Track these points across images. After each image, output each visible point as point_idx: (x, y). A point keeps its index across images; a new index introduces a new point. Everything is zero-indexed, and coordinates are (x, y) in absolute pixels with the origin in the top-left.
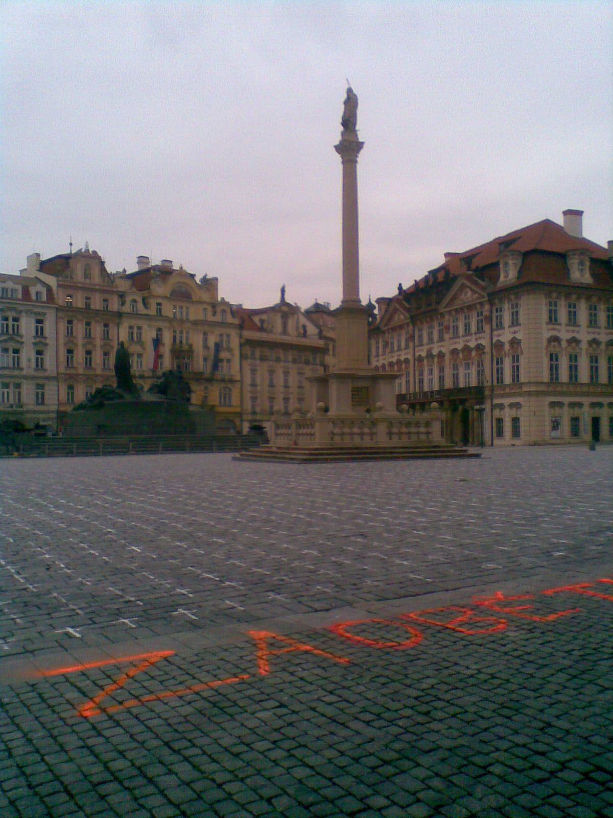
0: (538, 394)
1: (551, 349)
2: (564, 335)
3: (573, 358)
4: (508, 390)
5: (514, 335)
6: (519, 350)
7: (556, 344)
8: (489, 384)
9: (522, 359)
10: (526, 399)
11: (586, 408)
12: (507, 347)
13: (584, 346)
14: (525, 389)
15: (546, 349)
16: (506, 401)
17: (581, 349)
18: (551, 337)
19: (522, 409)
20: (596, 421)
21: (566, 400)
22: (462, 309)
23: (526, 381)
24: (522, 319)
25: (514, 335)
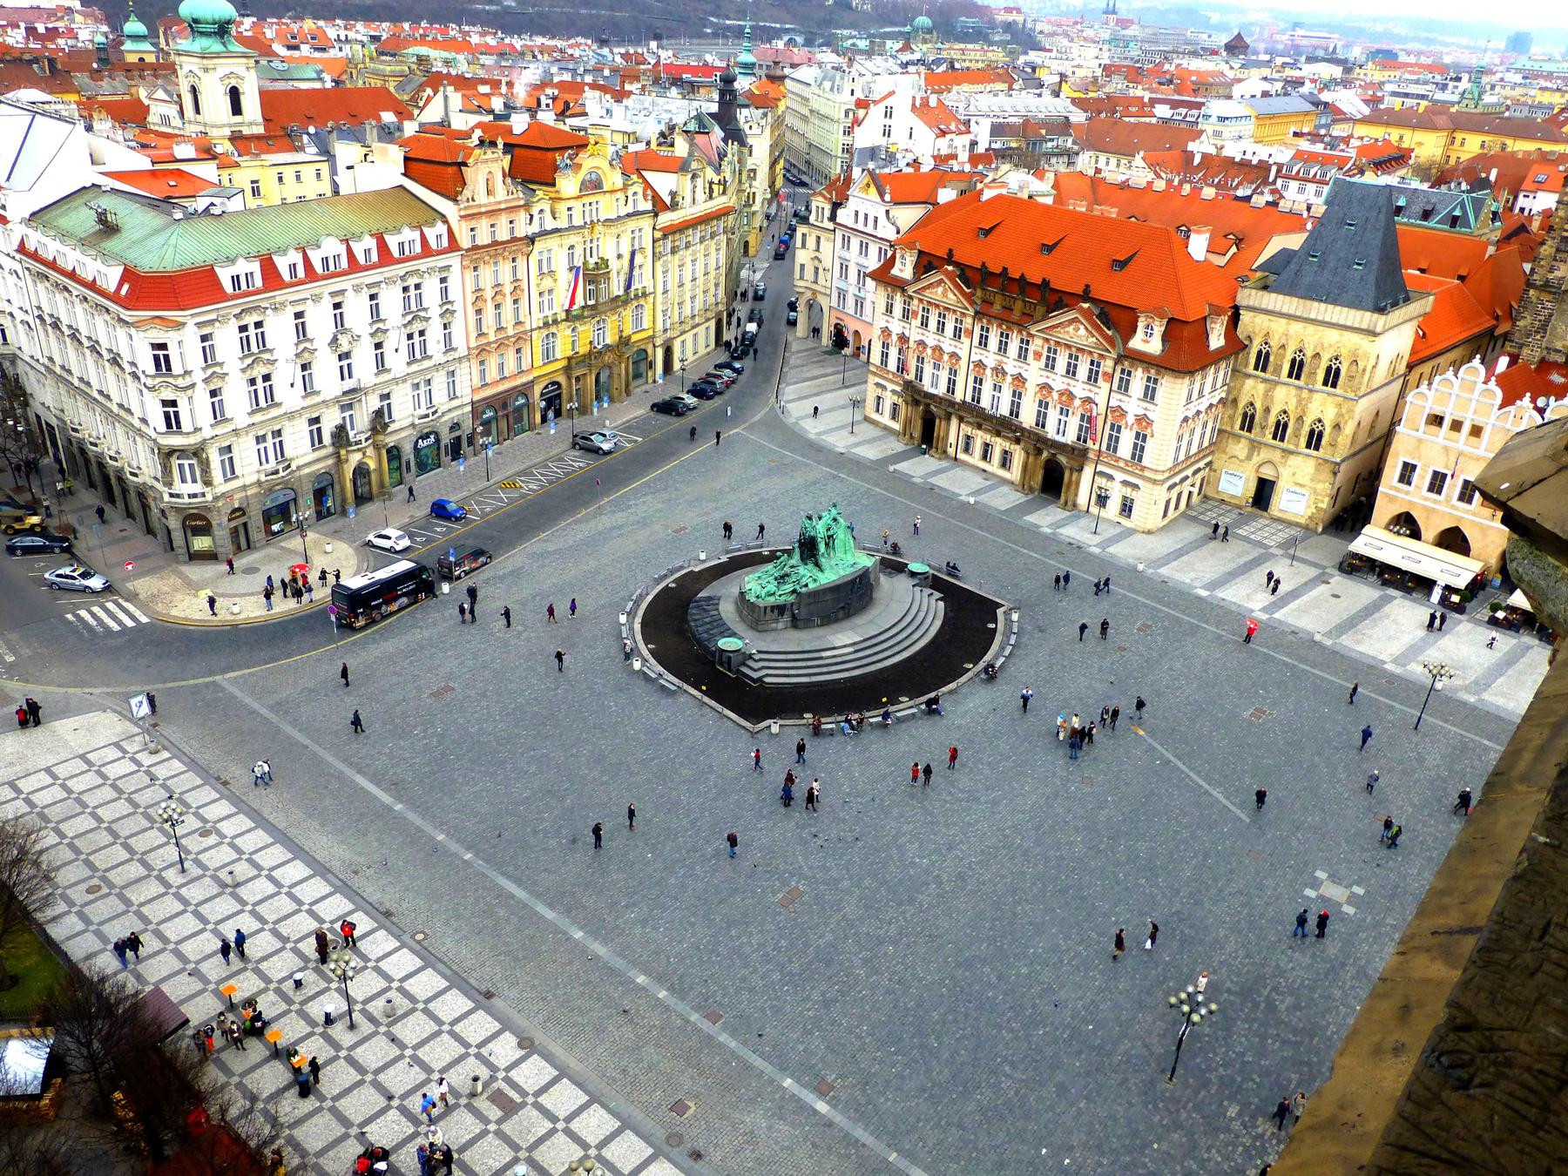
4: (1122, 464)
8: (1096, 447)
12: (1131, 419)
16: (1119, 476)
22: (1068, 346)
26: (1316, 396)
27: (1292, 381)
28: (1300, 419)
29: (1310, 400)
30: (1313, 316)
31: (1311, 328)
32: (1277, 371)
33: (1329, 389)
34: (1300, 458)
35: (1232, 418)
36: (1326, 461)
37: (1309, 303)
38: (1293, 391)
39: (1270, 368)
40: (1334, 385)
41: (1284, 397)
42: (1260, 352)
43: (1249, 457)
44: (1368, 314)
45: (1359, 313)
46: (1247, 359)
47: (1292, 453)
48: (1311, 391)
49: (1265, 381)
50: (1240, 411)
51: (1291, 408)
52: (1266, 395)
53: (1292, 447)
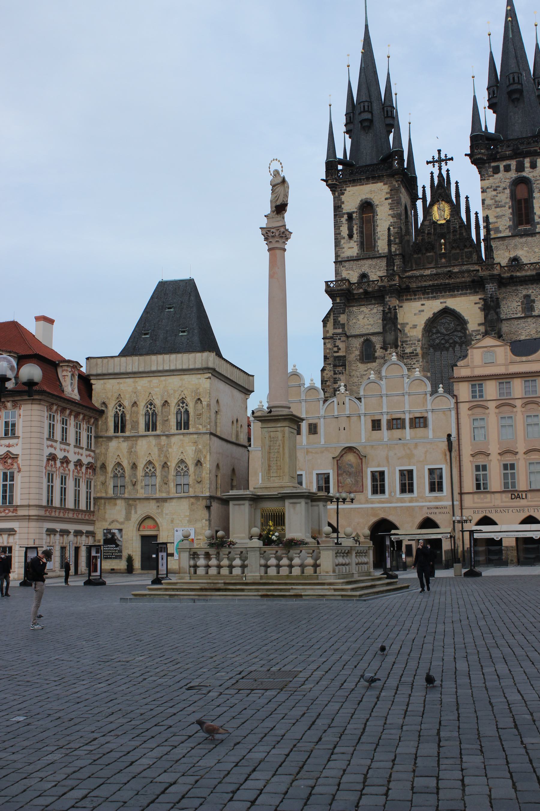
0: (40, 519)
1: (48, 468)
2: (60, 455)
3: (63, 480)
5: (8, 449)
6: (15, 466)
7: (53, 463)
9: (18, 478)
10: (25, 524)
11: (71, 537)
13: (71, 466)
14: (21, 512)
15: (45, 468)
17: (69, 470)
18: (51, 454)
19: (17, 536)
20: (77, 549)
21: (58, 526)
23: (25, 503)
24: (19, 431)
25: (8, 449)
26: (174, 439)
27: (150, 433)
28: (165, 465)
29: (169, 445)
30: (154, 368)
31: (155, 381)
32: (135, 426)
33: (183, 431)
34: (174, 503)
35: (104, 484)
36: (197, 497)
37: (148, 358)
38: (153, 441)
39: (128, 427)
40: (187, 426)
41: (146, 448)
42: (116, 415)
43: (128, 518)
44: (199, 355)
45: (192, 355)
46: (106, 422)
47: (165, 500)
48: (167, 436)
49: (127, 438)
50: (110, 474)
51: (155, 457)
52: (130, 452)
53: (164, 495)
